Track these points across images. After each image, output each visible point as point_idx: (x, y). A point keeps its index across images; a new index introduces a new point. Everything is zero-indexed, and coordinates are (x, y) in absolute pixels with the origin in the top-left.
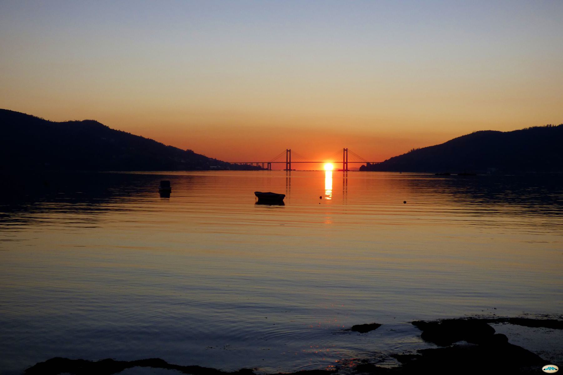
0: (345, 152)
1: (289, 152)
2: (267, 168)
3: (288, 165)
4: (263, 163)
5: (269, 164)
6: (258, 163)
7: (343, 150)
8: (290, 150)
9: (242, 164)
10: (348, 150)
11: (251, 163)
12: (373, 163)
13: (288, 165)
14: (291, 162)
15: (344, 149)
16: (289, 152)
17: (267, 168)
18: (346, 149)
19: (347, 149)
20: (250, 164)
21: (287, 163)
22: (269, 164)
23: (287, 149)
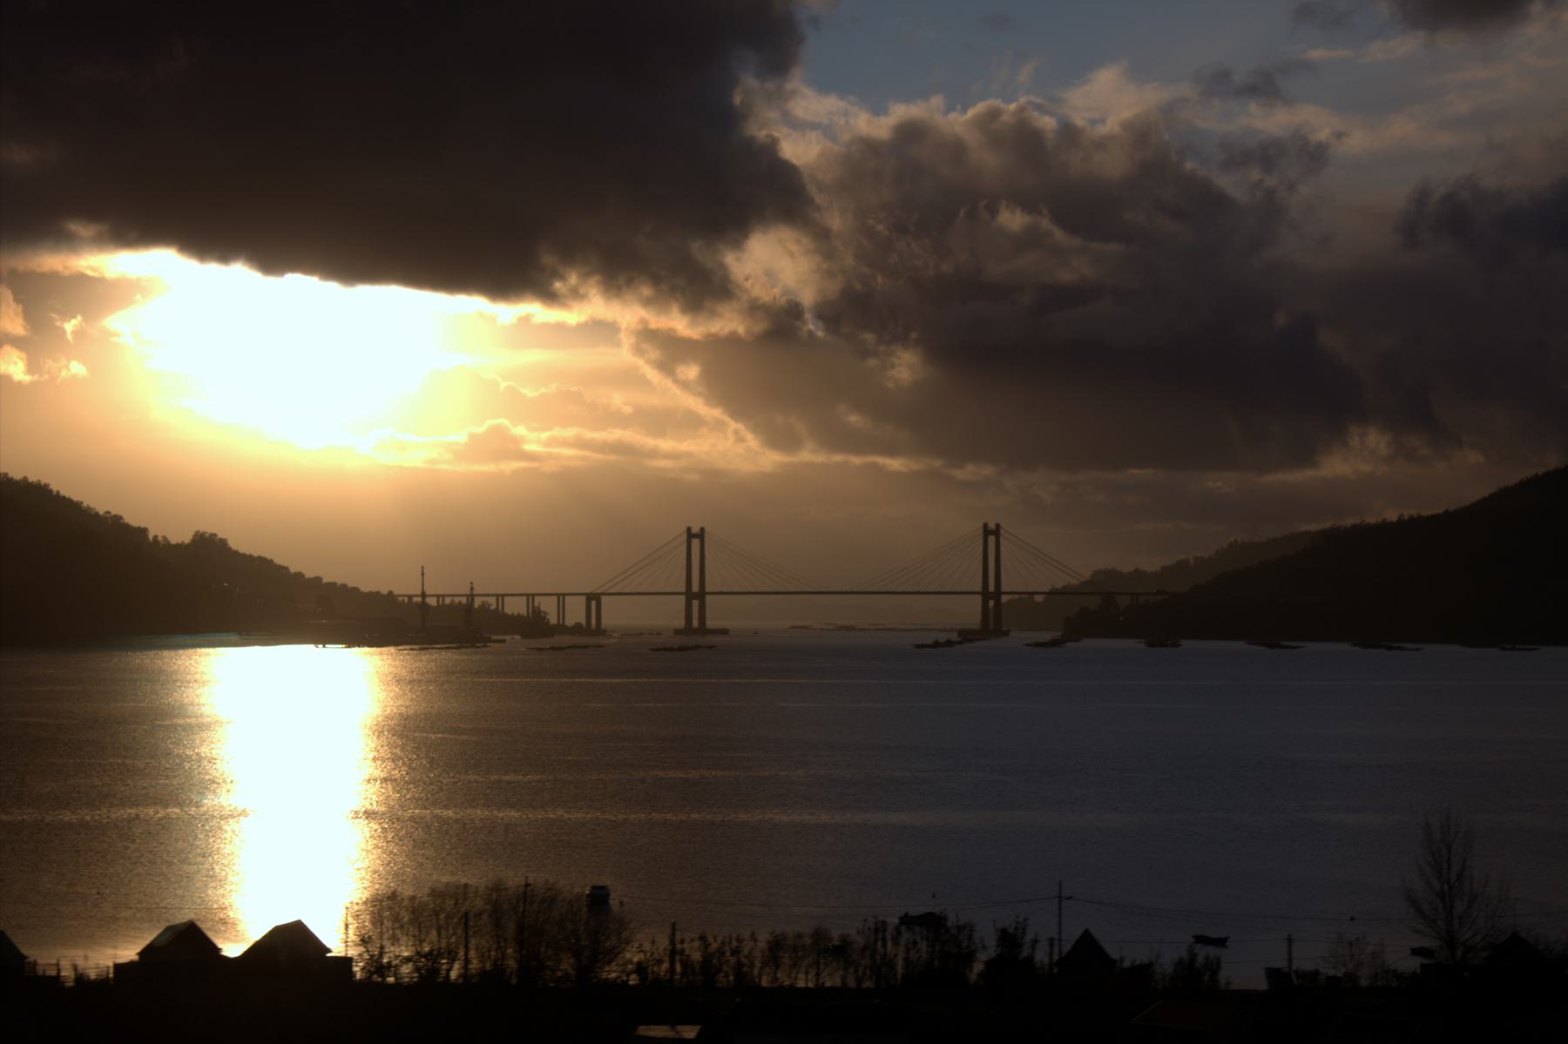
1: (696, 543)
3: (695, 603)
4: (561, 597)
5: (593, 603)
6: (533, 595)
8: (702, 530)
9: (448, 601)
10: (1002, 532)
14: (708, 589)
15: (985, 526)
16: (696, 543)
18: (992, 526)
19: (998, 526)
21: (690, 596)
22: (593, 603)
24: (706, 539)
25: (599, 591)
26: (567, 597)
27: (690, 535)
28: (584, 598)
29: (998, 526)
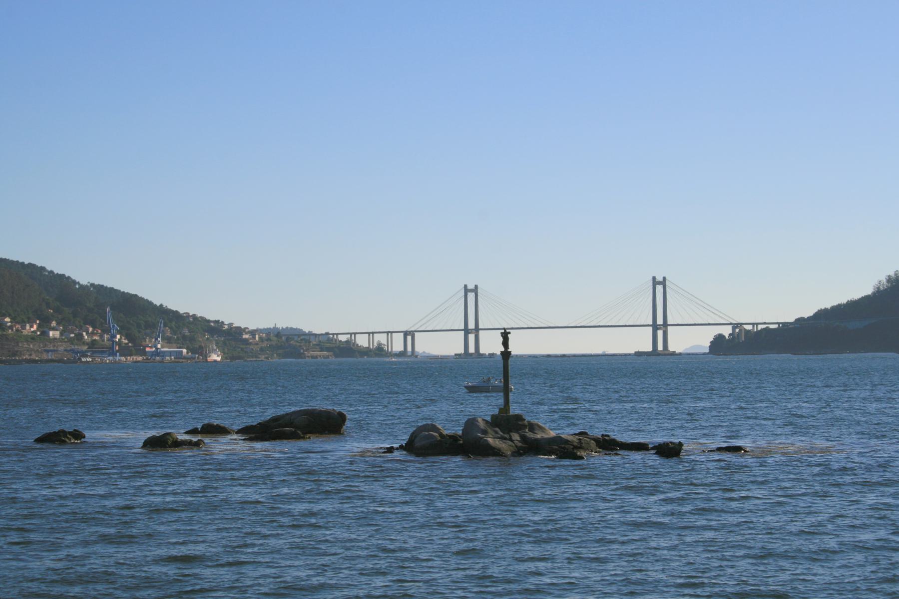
0: (659, 288)
1: (471, 296)
2: (402, 349)
3: (472, 337)
5: (409, 338)
7: (651, 283)
10: (667, 283)
11: (351, 334)
12: (753, 324)
13: (472, 337)
17: (402, 349)
19: (664, 278)
20: (349, 336)
22: (409, 338)
23: (466, 286)
24: (479, 294)
25: (413, 329)
26: (393, 334)
27: (466, 290)
28: (402, 334)
29: (664, 278)
